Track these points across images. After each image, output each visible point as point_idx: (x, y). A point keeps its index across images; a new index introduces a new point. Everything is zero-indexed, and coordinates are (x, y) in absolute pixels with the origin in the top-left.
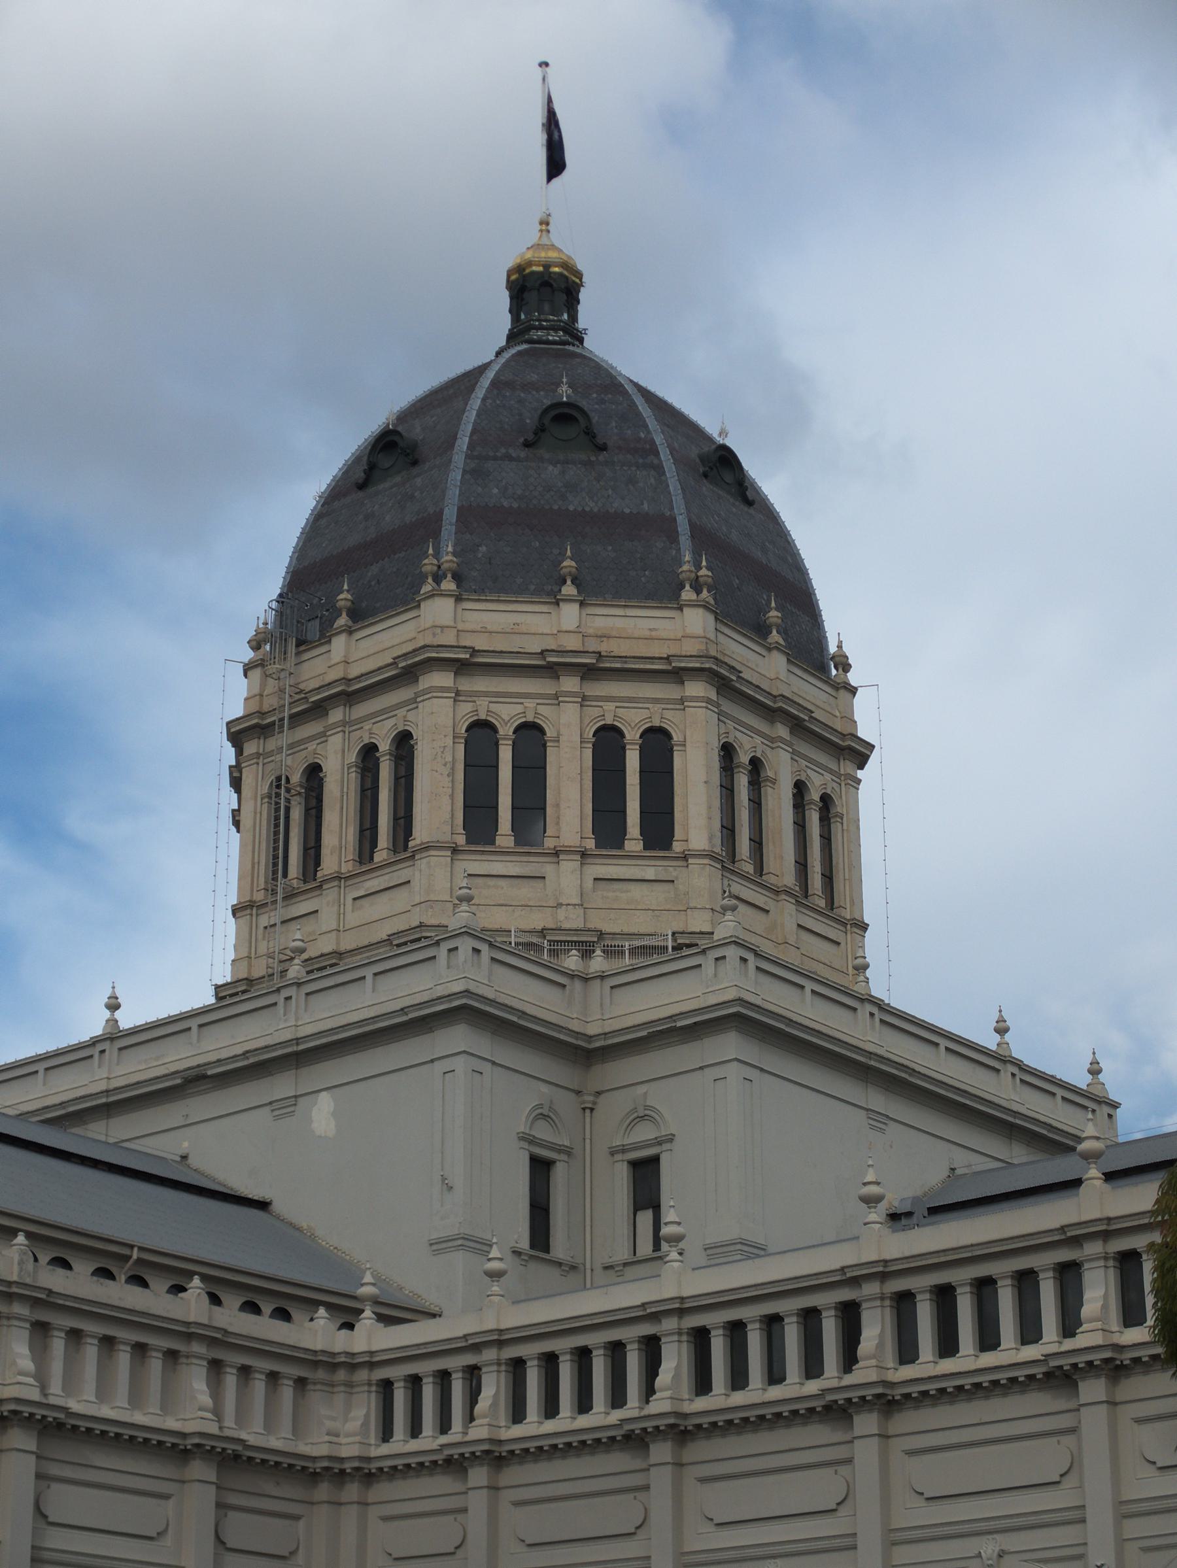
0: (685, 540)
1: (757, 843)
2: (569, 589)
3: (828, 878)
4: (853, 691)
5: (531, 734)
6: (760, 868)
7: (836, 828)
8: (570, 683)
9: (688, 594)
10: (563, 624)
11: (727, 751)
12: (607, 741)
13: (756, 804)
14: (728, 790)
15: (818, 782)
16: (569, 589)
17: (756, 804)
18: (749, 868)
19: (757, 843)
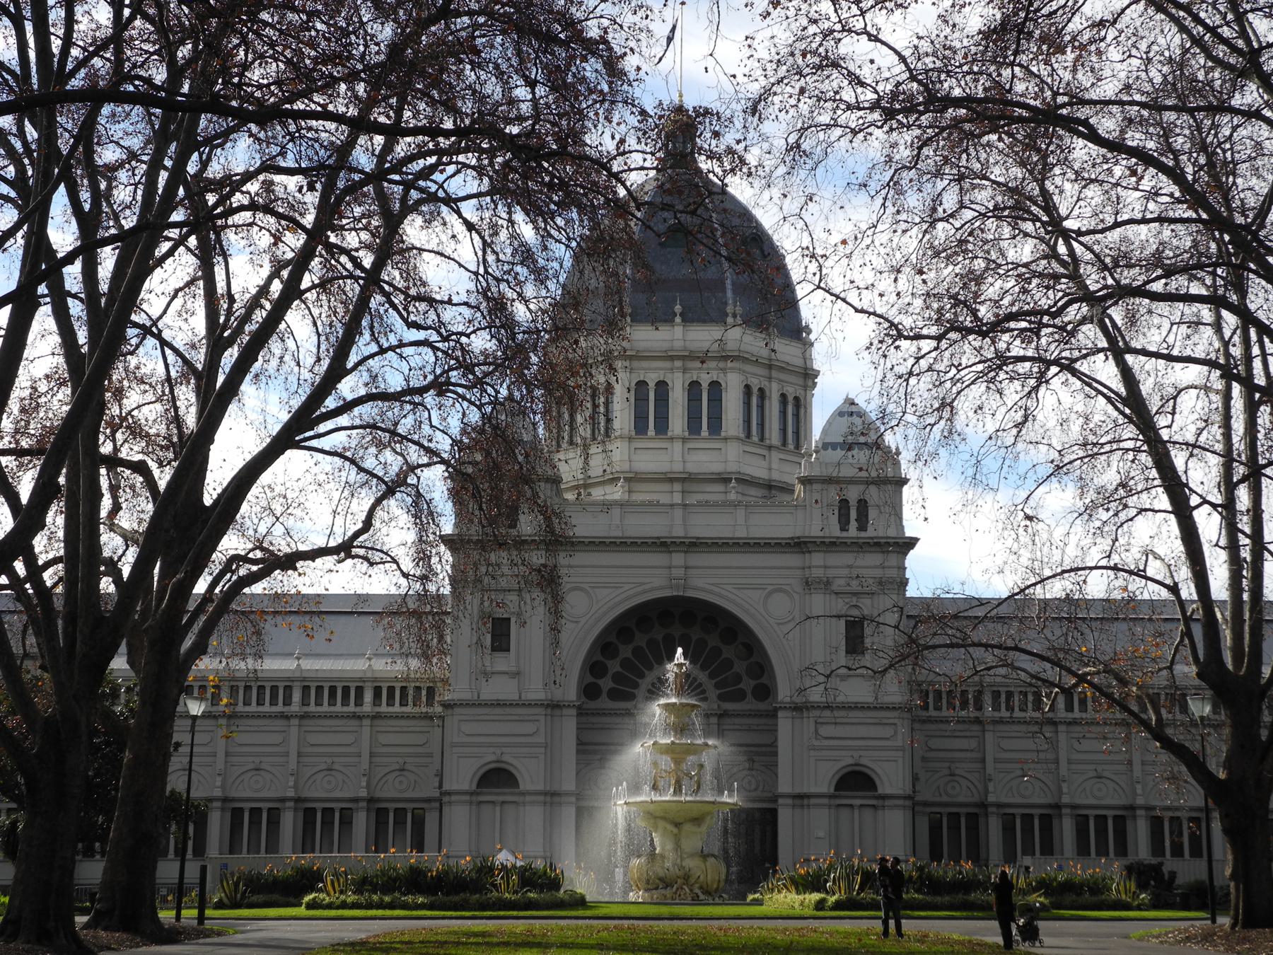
0: (729, 294)
1: (761, 425)
2: (678, 319)
3: (797, 433)
4: (812, 345)
5: (662, 386)
6: (762, 439)
7: (802, 411)
8: (678, 364)
9: (730, 320)
10: (674, 335)
11: (747, 387)
12: (694, 387)
13: (761, 407)
14: (747, 404)
15: (790, 391)
16: (678, 319)
17: (761, 407)
18: (755, 439)
19: (761, 425)
